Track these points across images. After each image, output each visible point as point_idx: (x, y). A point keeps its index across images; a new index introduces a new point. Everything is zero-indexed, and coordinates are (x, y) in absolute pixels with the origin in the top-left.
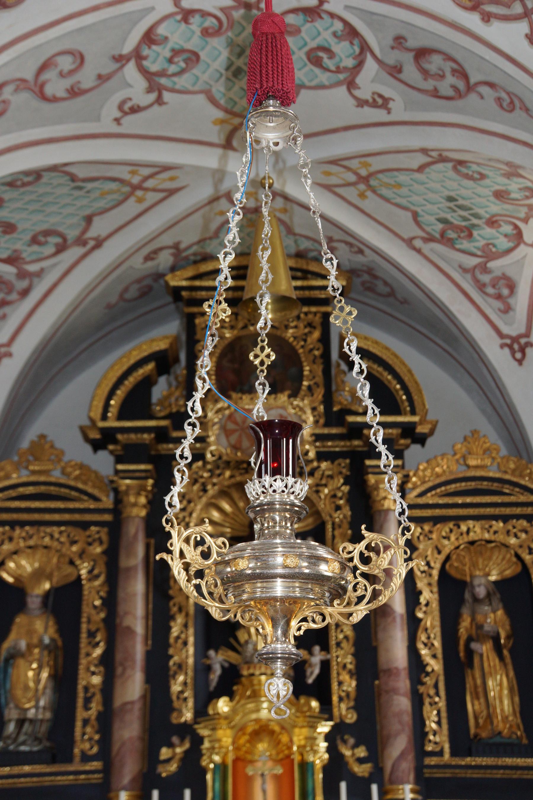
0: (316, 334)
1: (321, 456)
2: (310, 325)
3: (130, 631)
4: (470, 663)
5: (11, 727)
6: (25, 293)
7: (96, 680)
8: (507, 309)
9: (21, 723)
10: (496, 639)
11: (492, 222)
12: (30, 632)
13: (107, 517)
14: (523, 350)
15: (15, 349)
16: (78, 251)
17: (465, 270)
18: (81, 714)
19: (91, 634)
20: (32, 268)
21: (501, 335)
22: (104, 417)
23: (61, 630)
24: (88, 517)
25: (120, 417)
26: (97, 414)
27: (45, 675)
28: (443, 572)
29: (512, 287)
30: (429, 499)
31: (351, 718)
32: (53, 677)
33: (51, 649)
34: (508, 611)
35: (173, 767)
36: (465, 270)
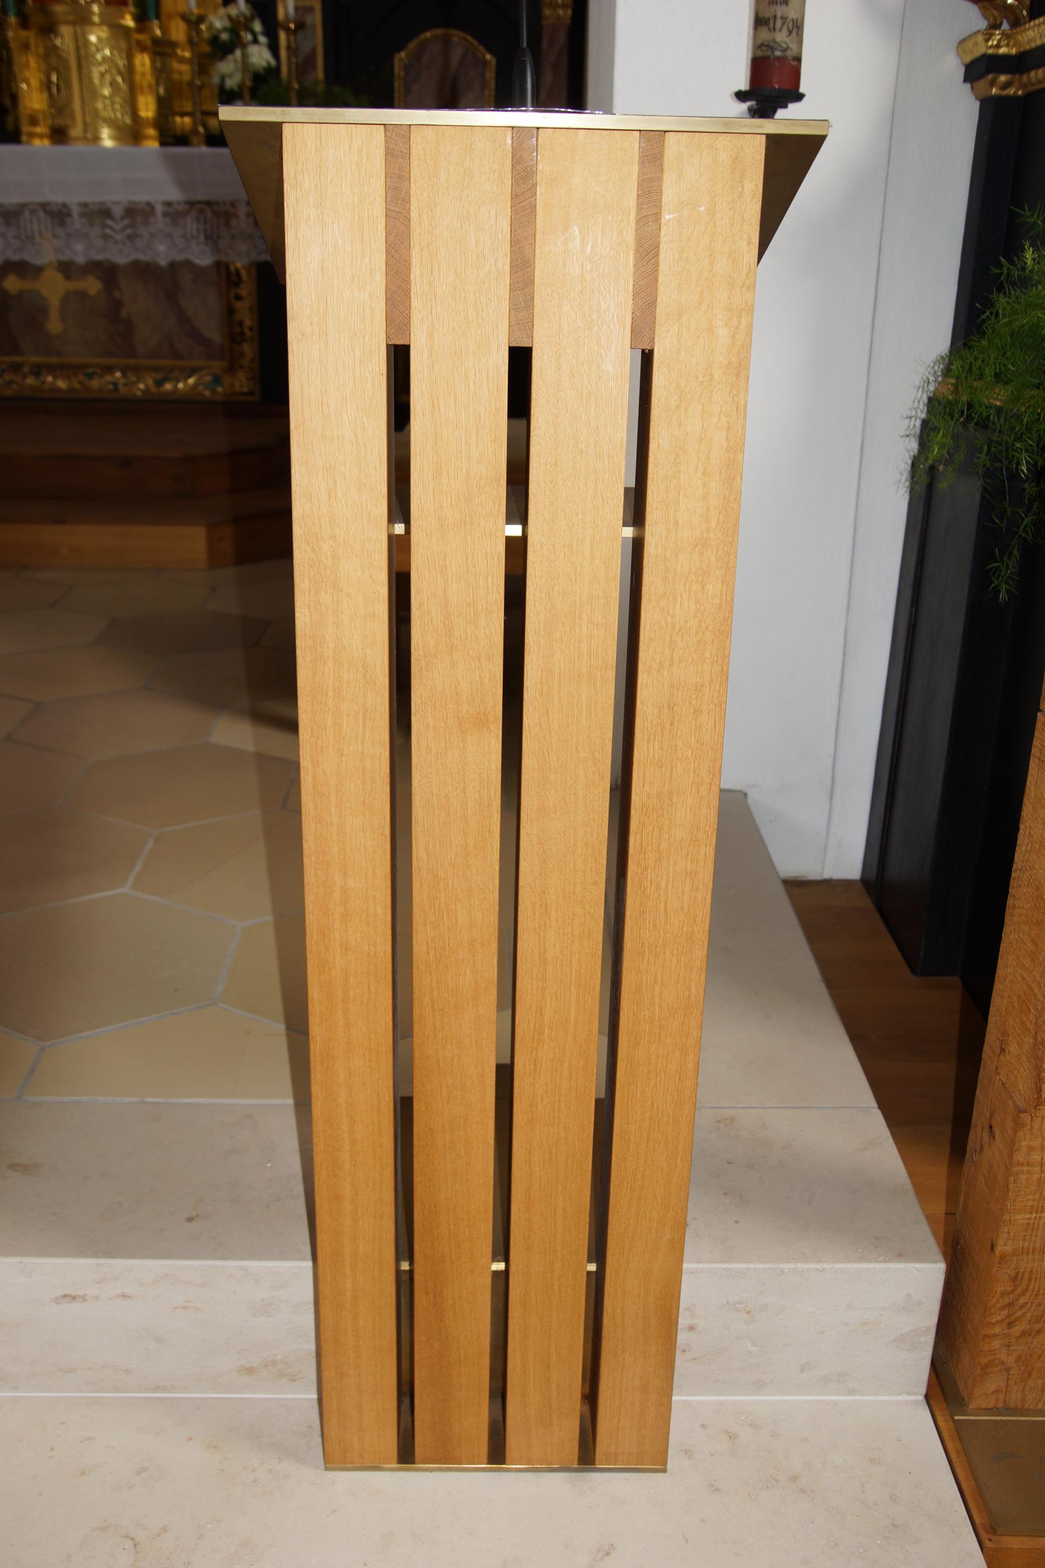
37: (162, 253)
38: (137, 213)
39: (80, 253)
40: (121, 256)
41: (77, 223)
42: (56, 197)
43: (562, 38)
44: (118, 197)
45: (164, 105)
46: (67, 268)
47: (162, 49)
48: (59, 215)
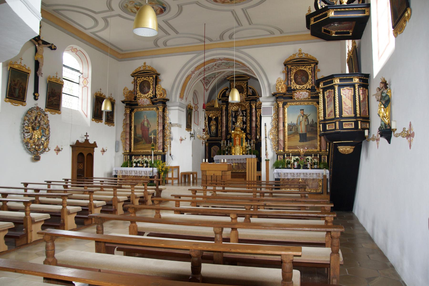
1: (246, 101)
2: (245, 84)
5: (211, 133)
6: (209, 83)
7: (220, 128)
9: (212, 133)
12: (213, 123)
13: (221, 109)
15: (209, 89)
16: (215, 78)
18: (219, 132)
19: (219, 123)
20: (210, 80)
22: (219, 98)
23: (216, 123)
24: (219, 109)
25: (221, 98)
27: (215, 127)
30: (259, 106)
31: (249, 132)
32: (216, 128)
33: (215, 125)
35: (229, 137)
37: (242, 162)
38: (240, 159)
39: (236, 162)
40: (239, 162)
41: (236, 160)
44: (239, 158)
45: (243, 152)
46: (235, 163)
47: (243, 148)
48: (235, 159)
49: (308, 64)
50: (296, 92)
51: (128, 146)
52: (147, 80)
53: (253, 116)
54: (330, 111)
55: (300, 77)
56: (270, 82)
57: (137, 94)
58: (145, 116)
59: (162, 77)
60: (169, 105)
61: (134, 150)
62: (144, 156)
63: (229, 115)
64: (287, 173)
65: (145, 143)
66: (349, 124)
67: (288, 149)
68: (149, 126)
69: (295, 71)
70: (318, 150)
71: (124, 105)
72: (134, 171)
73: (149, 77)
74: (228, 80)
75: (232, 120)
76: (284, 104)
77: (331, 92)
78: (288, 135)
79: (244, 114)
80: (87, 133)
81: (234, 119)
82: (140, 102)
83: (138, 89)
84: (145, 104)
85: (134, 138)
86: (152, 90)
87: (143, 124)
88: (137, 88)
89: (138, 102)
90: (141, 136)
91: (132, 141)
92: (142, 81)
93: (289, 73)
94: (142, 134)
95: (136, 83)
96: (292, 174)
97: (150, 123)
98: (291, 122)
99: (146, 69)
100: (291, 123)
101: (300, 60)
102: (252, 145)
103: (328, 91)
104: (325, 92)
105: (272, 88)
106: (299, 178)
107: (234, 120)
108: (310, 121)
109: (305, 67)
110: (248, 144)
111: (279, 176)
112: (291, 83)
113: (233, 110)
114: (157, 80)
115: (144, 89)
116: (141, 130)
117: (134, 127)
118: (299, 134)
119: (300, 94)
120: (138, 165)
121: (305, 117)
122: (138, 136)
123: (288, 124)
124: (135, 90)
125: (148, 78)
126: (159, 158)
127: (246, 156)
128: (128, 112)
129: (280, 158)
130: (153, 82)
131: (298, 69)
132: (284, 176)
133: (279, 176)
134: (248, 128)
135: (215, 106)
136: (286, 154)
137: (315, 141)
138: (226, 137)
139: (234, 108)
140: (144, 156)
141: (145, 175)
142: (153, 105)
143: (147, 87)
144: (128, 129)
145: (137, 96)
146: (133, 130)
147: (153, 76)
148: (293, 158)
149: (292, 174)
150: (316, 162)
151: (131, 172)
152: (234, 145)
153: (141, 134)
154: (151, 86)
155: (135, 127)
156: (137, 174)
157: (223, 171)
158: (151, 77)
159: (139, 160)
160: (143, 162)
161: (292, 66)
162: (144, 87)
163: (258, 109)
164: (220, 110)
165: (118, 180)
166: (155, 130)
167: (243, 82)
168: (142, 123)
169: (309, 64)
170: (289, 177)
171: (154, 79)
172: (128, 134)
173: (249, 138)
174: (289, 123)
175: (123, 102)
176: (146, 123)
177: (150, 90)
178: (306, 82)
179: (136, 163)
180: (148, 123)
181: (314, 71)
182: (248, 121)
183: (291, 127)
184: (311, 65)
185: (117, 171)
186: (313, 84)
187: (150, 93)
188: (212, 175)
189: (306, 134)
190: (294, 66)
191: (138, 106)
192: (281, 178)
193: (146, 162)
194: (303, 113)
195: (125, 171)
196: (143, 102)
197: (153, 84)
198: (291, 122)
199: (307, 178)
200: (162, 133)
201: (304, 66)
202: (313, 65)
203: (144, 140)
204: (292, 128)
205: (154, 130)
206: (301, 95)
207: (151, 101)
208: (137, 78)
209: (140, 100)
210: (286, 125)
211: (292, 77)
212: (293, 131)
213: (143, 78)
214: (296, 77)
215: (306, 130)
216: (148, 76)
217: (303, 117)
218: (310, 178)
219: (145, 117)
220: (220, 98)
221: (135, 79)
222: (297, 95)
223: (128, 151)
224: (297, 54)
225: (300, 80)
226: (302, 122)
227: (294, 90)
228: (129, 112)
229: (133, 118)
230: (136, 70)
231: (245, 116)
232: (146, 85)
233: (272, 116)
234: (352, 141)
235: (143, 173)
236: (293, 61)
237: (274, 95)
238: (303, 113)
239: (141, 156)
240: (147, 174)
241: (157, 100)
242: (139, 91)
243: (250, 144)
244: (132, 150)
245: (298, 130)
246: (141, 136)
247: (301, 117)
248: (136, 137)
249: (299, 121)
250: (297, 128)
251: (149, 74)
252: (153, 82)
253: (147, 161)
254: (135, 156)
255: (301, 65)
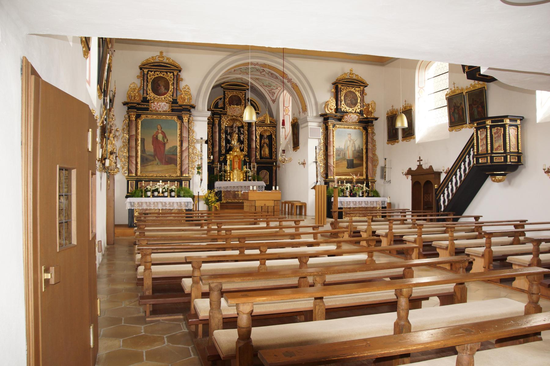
0: (244, 96)
3: (216, 141)
4: (263, 147)
8: (273, 96)
10: (267, 144)
11: (274, 86)
13: (212, 123)
14: (274, 102)
17: (268, 90)
21: (271, 99)
26: (212, 108)
28: (260, 134)
29: (274, 93)
30: (259, 123)
34: (269, 140)
35: (222, 159)
36: (268, 90)
42: (241, 185)
43: (275, 171)
49: (357, 86)
50: (347, 115)
51: (134, 166)
52: (164, 76)
53: (253, 134)
54: (498, 146)
55: (349, 99)
56: (318, 100)
57: (147, 94)
58: (159, 126)
59: (183, 75)
60: (195, 115)
61: (141, 173)
62: (169, 182)
63: (222, 131)
64: (350, 202)
65: (159, 163)
66: (514, 158)
67: (336, 176)
68: (166, 141)
69: (345, 91)
70: (364, 177)
71: (126, 108)
72: (162, 203)
73: (167, 72)
74: (222, 87)
75: (226, 137)
76: (334, 126)
77: (499, 129)
78: (336, 161)
79: (242, 132)
80: (420, 157)
81: (229, 137)
82: (154, 107)
83: (150, 87)
84: (160, 110)
85: (141, 155)
86: (172, 91)
87: (155, 136)
88: (147, 85)
89: (150, 106)
90: (153, 154)
91: (139, 160)
92: (156, 76)
93: (339, 93)
94: (154, 151)
95: (145, 78)
96: (354, 202)
97: (166, 136)
98: (339, 147)
99: (163, 61)
100: (338, 147)
101: (350, 80)
102: (252, 169)
103: (496, 128)
104: (493, 129)
105: (319, 106)
106: (360, 206)
107: (229, 139)
108: (357, 146)
109: (355, 89)
110: (247, 169)
111: (342, 205)
112: (341, 104)
113: (226, 125)
114: (178, 79)
115: (158, 88)
116: (153, 145)
117: (141, 141)
118: (346, 160)
119: (351, 117)
120: (156, 194)
121: (352, 142)
122: (148, 154)
123: (336, 149)
124: (145, 88)
125: (165, 73)
126: (185, 185)
127: (247, 183)
128: (134, 118)
129: (331, 185)
130: (173, 80)
131: (348, 90)
132: (347, 205)
133: (342, 205)
134: (246, 149)
135: (266, 122)
136: (340, 181)
137: (361, 167)
138: (219, 159)
139: (228, 124)
140: (169, 182)
141: (178, 208)
142: (172, 111)
143: (164, 86)
144: (133, 143)
145: (147, 97)
146: (140, 145)
147: (173, 73)
148: (349, 185)
149: (354, 202)
150: (368, 189)
151: (156, 203)
152: (232, 169)
153: (152, 150)
154: (171, 87)
155: (143, 140)
156: (166, 207)
157: (276, 200)
158: (170, 73)
159: (156, 188)
160: (164, 190)
161: (342, 86)
162: (159, 86)
163: (257, 126)
164: (211, 124)
165: (213, 214)
166: (175, 146)
167: (241, 92)
168: (153, 136)
169: (359, 86)
170: (352, 206)
171: (175, 77)
172: (134, 150)
173: (247, 160)
174: (337, 148)
175: (125, 104)
176: (160, 137)
177: (168, 91)
178: (355, 104)
179: (153, 191)
180: (164, 136)
181: (363, 93)
182: (246, 140)
183: (339, 152)
184: (360, 88)
185: (134, 202)
186: (361, 108)
187: (168, 96)
188: (263, 205)
189: (353, 160)
190: (344, 86)
191: (148, 111)
192: (344, 206)
193: (172, 191)
194: (350, 138)
195: (146, 203)
196: (159, 107)
197: (173, 83)
198: (339, 147)
199: (368, 206)
200: (187, 151)
201: (353, 87)
202: (362, 88)
203: (157, 160)
204: (340, 153)
205: (174, 147)
206: (351, 118)
207: (172, 106)
208: (148, 71)
209: (156, 103)
210: (335, 150)
211: (343, 98)
212: (341, 157)
213: (157, 73)
214: (346, 98)
215: (353, 157)
216: (165, 71)
217: (350, 141)
218: (371, 206)
219: (159, 128)
220: (213, 109)
221: (145, 73)
222: (347, 118)
223: (134, 175)
224: (349, 74)
225: (350, 102)
226: (349, 147)
227: (344, 112)
228: (135, 119)
229: (140, 128)
230: (147, 59)
231: (242, 134)
232: (162, 83)
233: (319, 139)
234: (503, 172)
235: (175, 205)
236: (344, 80)
237: (322, 115)
238: (350, 138)
239: (161, 181)
240: (181, 206)
241: (181, 106)
242: (151, 91)
243: (250, 169)
244: (139, 174)
245: (346, 155)
246: (153, 154)
247: (349, 142)
248: (142, 154)
249: (346, 146)
250: (345, 154)
251: (169, 68)
252: (173, 80)
253: (170, 189)
254: (153, 181)
255: (350, 86)
